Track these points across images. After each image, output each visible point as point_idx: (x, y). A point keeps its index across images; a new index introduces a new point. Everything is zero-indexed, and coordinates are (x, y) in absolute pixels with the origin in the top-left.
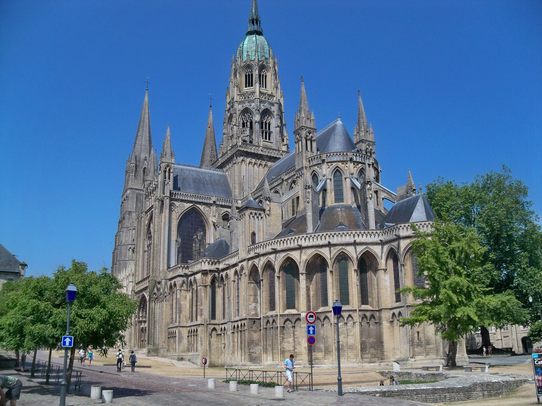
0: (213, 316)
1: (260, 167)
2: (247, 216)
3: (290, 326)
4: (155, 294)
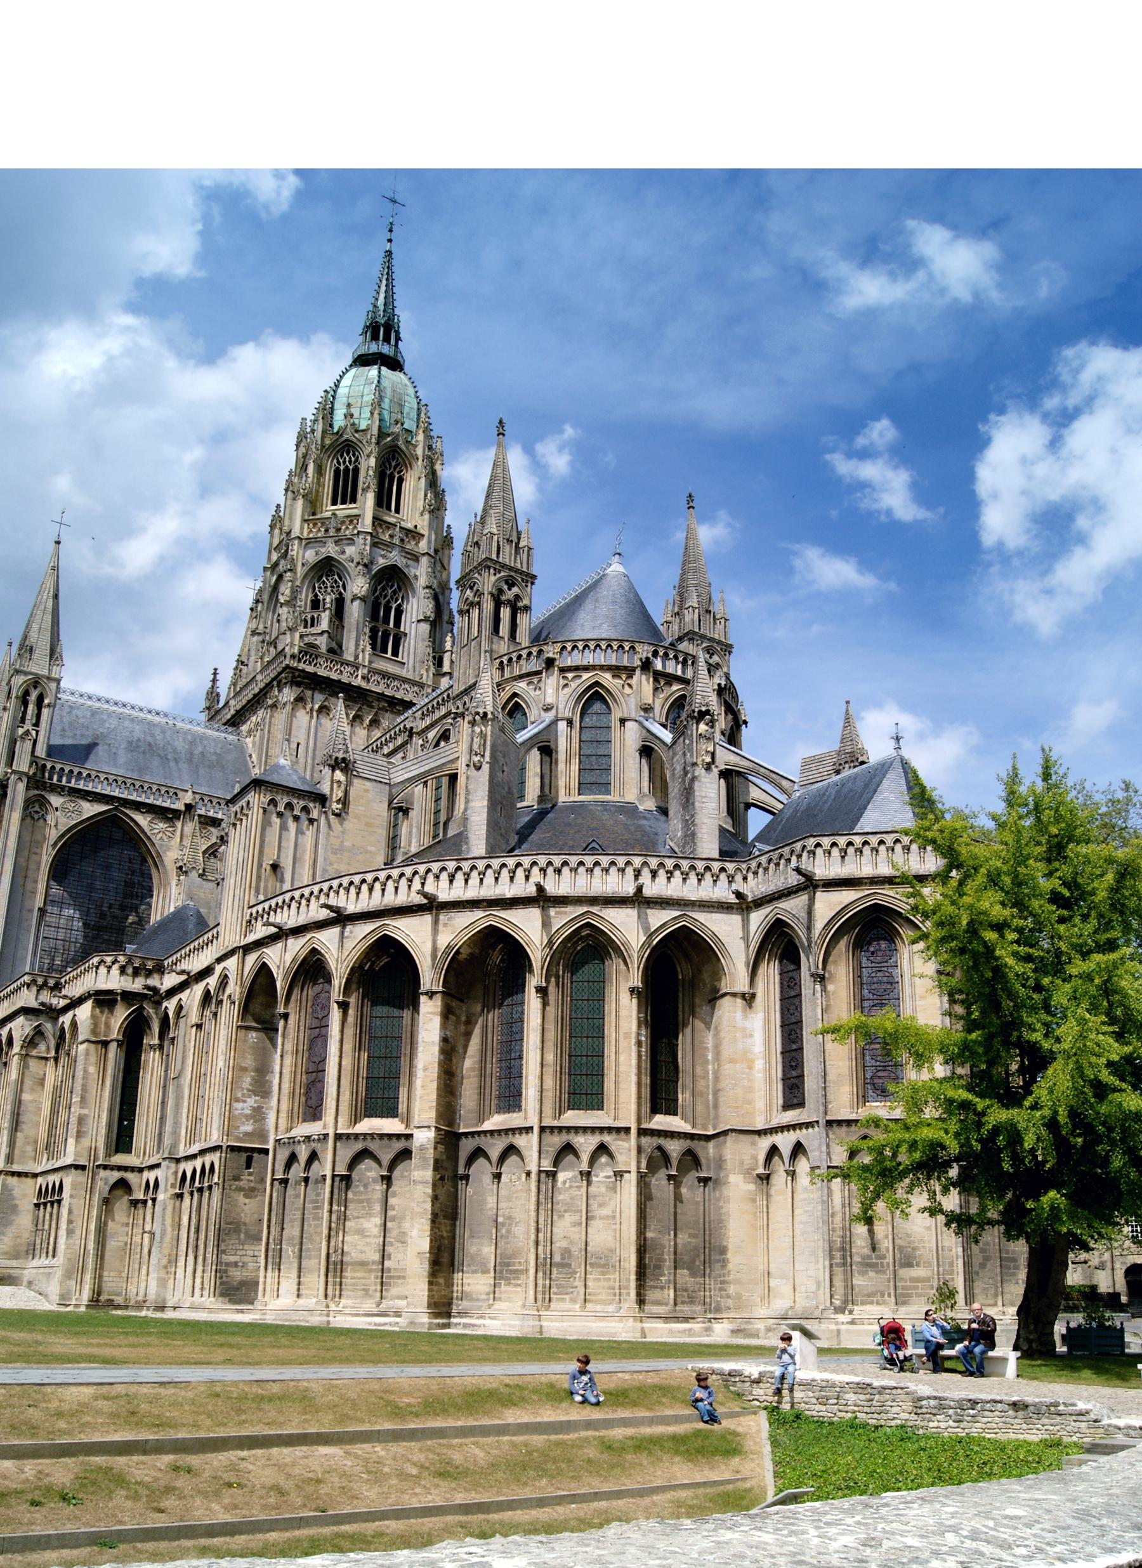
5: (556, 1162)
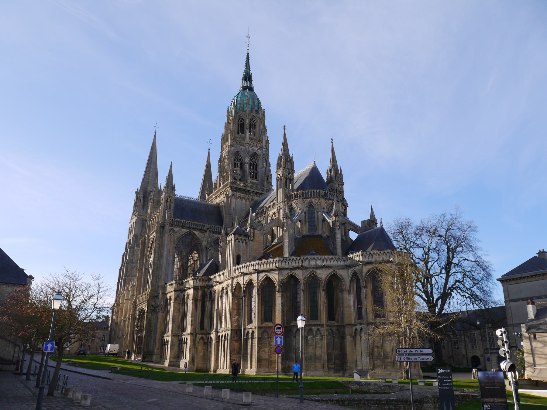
0: (202, 327)
3: (266, 337)
4: (153, 306)
5: (308, 334)
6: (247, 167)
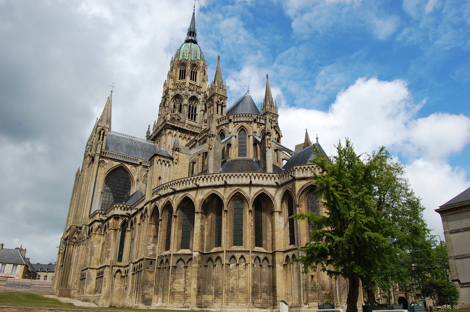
1: (184, 139)
2: (155, 162)
3: (183, 266)
4: (75, 238)
6: (185, 109)
